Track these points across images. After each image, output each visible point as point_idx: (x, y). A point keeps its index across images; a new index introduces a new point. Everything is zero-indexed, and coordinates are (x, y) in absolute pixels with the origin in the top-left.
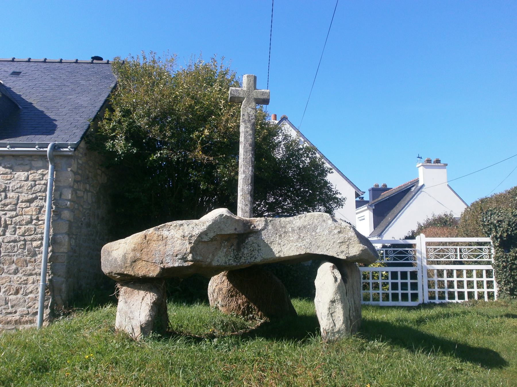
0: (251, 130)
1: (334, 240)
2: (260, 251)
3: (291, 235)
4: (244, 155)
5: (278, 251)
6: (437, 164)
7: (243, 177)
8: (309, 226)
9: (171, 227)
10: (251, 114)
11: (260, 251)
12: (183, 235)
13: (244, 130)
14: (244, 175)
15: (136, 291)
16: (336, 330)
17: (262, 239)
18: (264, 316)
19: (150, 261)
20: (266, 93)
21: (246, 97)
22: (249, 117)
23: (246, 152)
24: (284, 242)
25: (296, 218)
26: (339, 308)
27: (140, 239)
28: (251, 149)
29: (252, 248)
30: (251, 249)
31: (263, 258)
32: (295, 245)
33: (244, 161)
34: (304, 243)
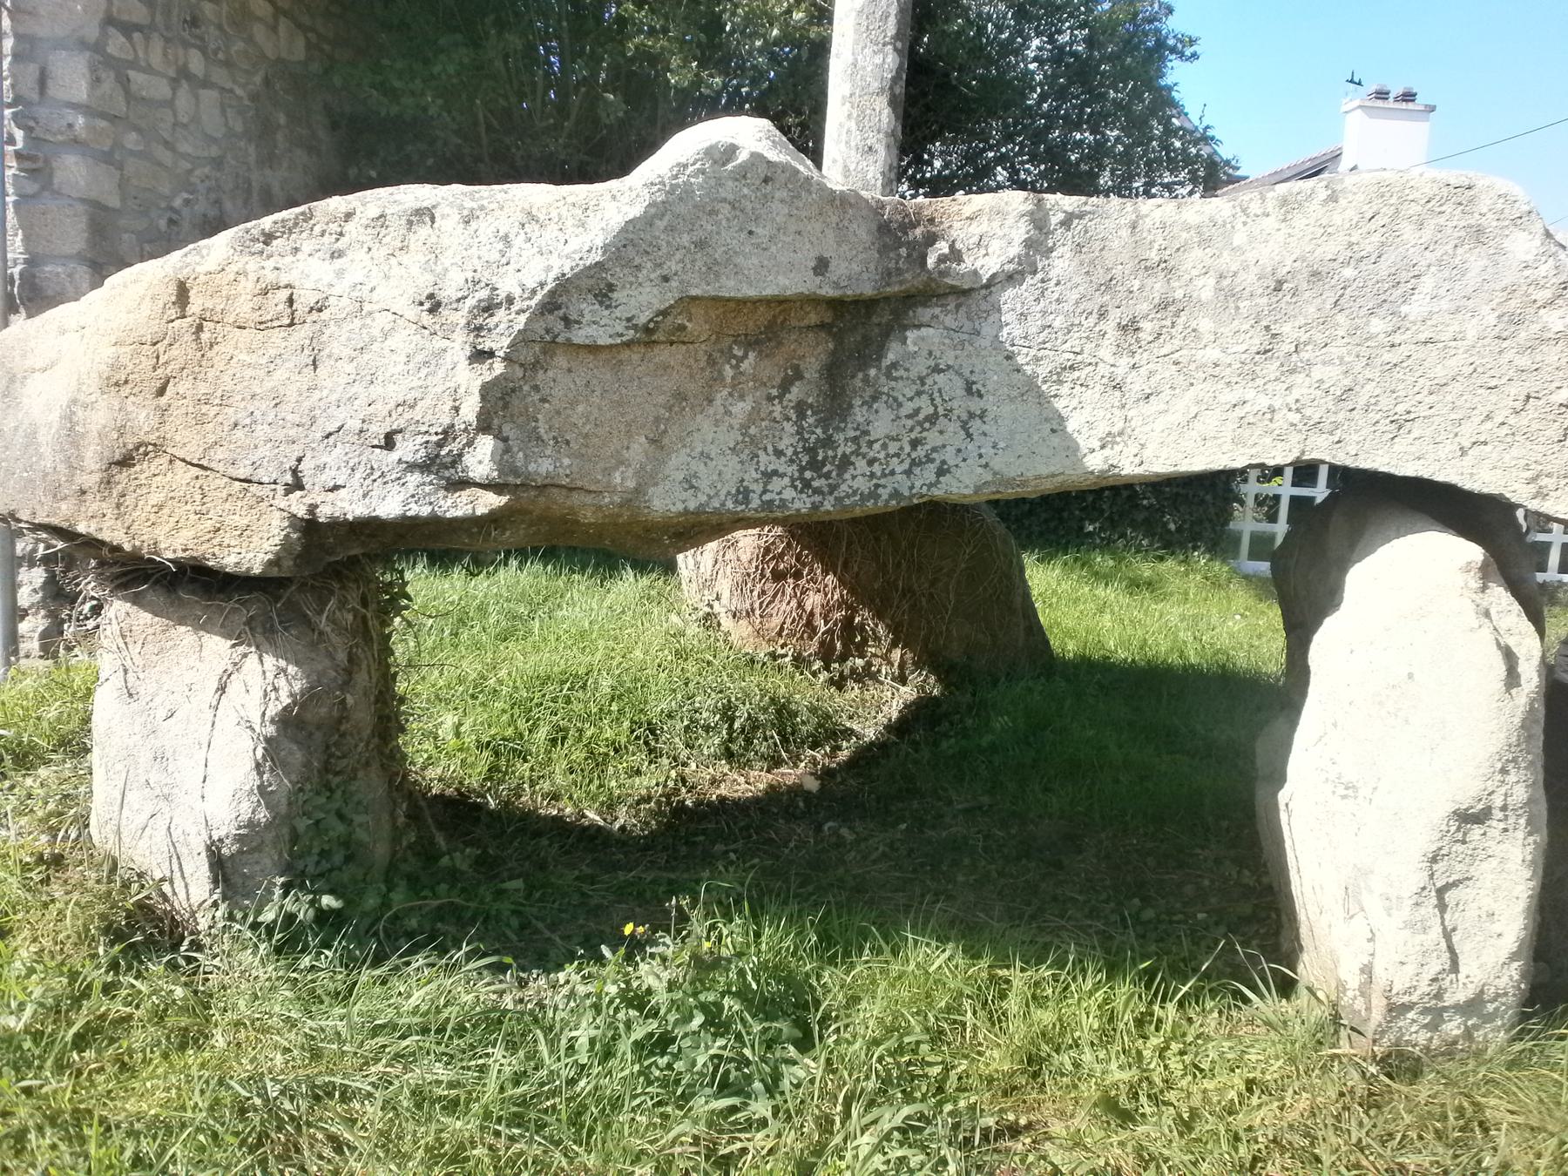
1: (1531, 385)
2: (976, 425)
3: (1205, 325)
5: (1102, 429)
6: (1404, 105)
8: (1348, 272)
9: (349, 227)
11: (976, 425)
12: (431, 296)
15: (184, 635)
16: (1459, 994)
17: (997, 343)
18: (918, 665)
19: (221, 467)
24: (1151, 374)
25: (1255, 208)
26: (1503, 860)
27: (146, 309)
29: (924, 403)
30: (917, 411)
31: (995, 474)
32: (1230, 397)
34: (1296, 394)
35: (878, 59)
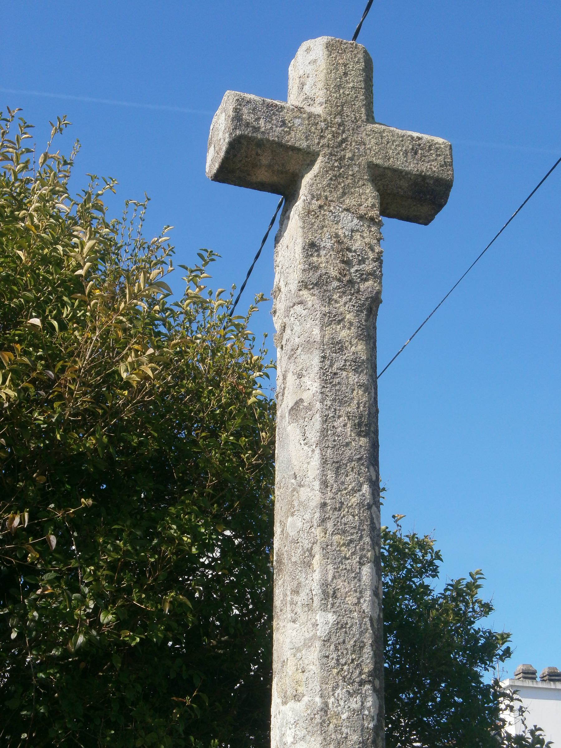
0: (358, 337)
4: (325, 484)
6: (552, 685)
7: (322, 631)
10: (357, 244)
13: (316, 331)
14: (331, 618)
20: (431, 146)
21: (326, 150)
22: (348, 263)
23: (338, 468)
28: (364, 453)
33: (323, 521)
35: (355, 703)
